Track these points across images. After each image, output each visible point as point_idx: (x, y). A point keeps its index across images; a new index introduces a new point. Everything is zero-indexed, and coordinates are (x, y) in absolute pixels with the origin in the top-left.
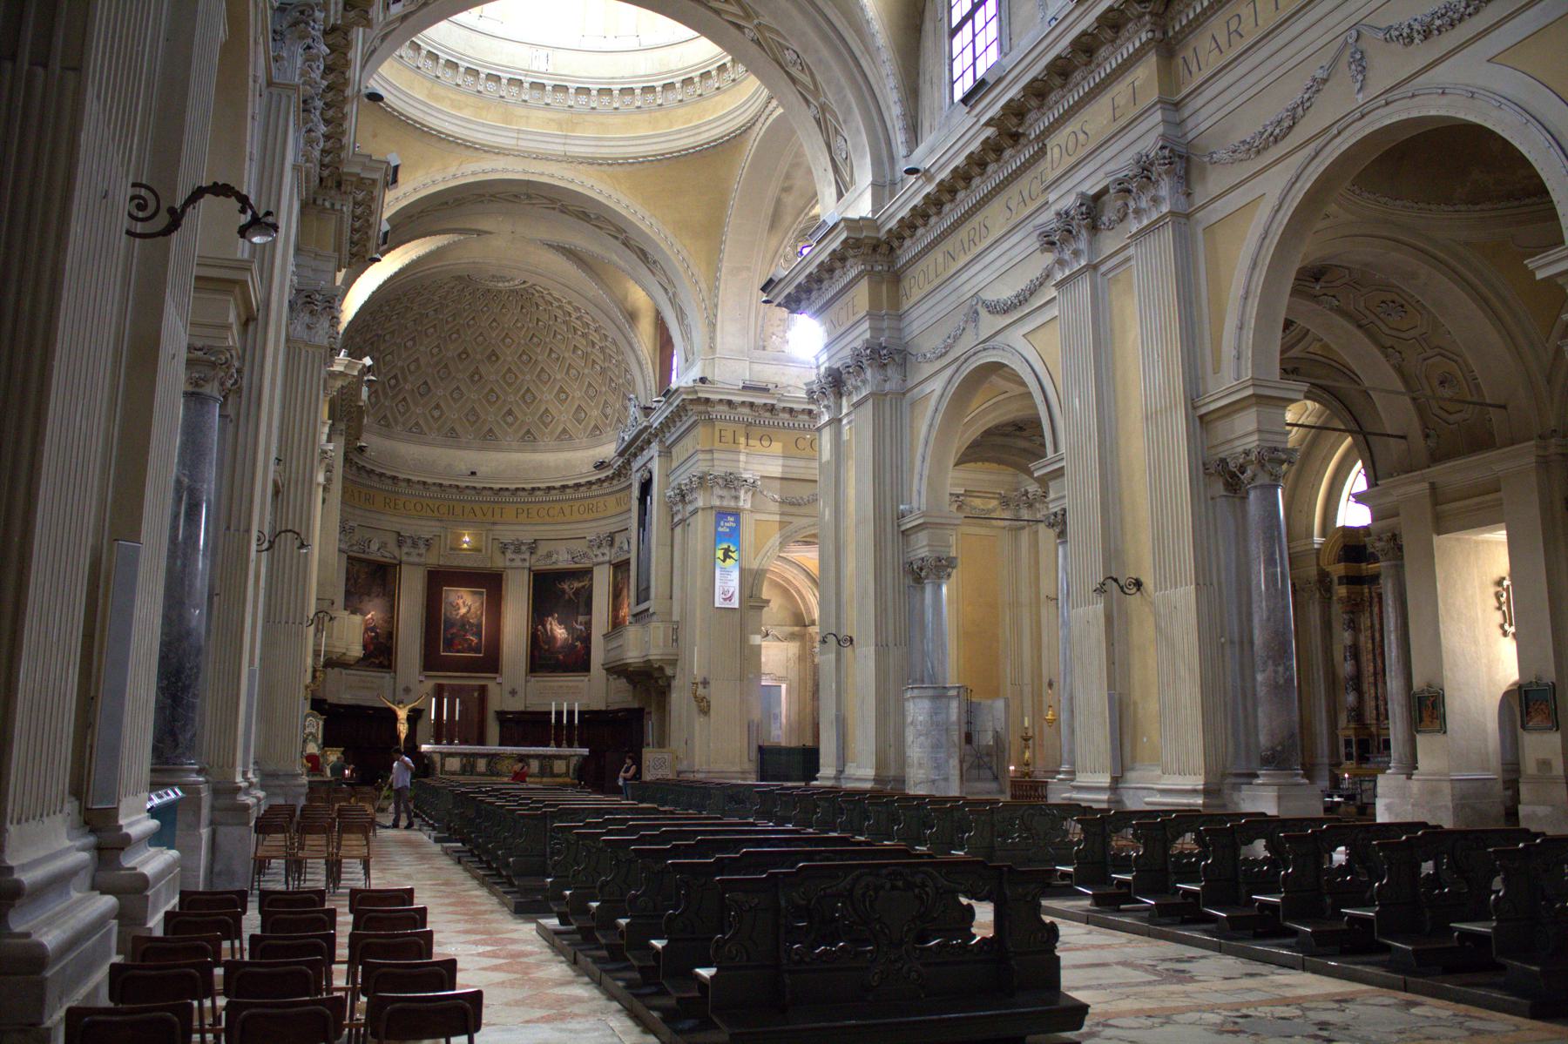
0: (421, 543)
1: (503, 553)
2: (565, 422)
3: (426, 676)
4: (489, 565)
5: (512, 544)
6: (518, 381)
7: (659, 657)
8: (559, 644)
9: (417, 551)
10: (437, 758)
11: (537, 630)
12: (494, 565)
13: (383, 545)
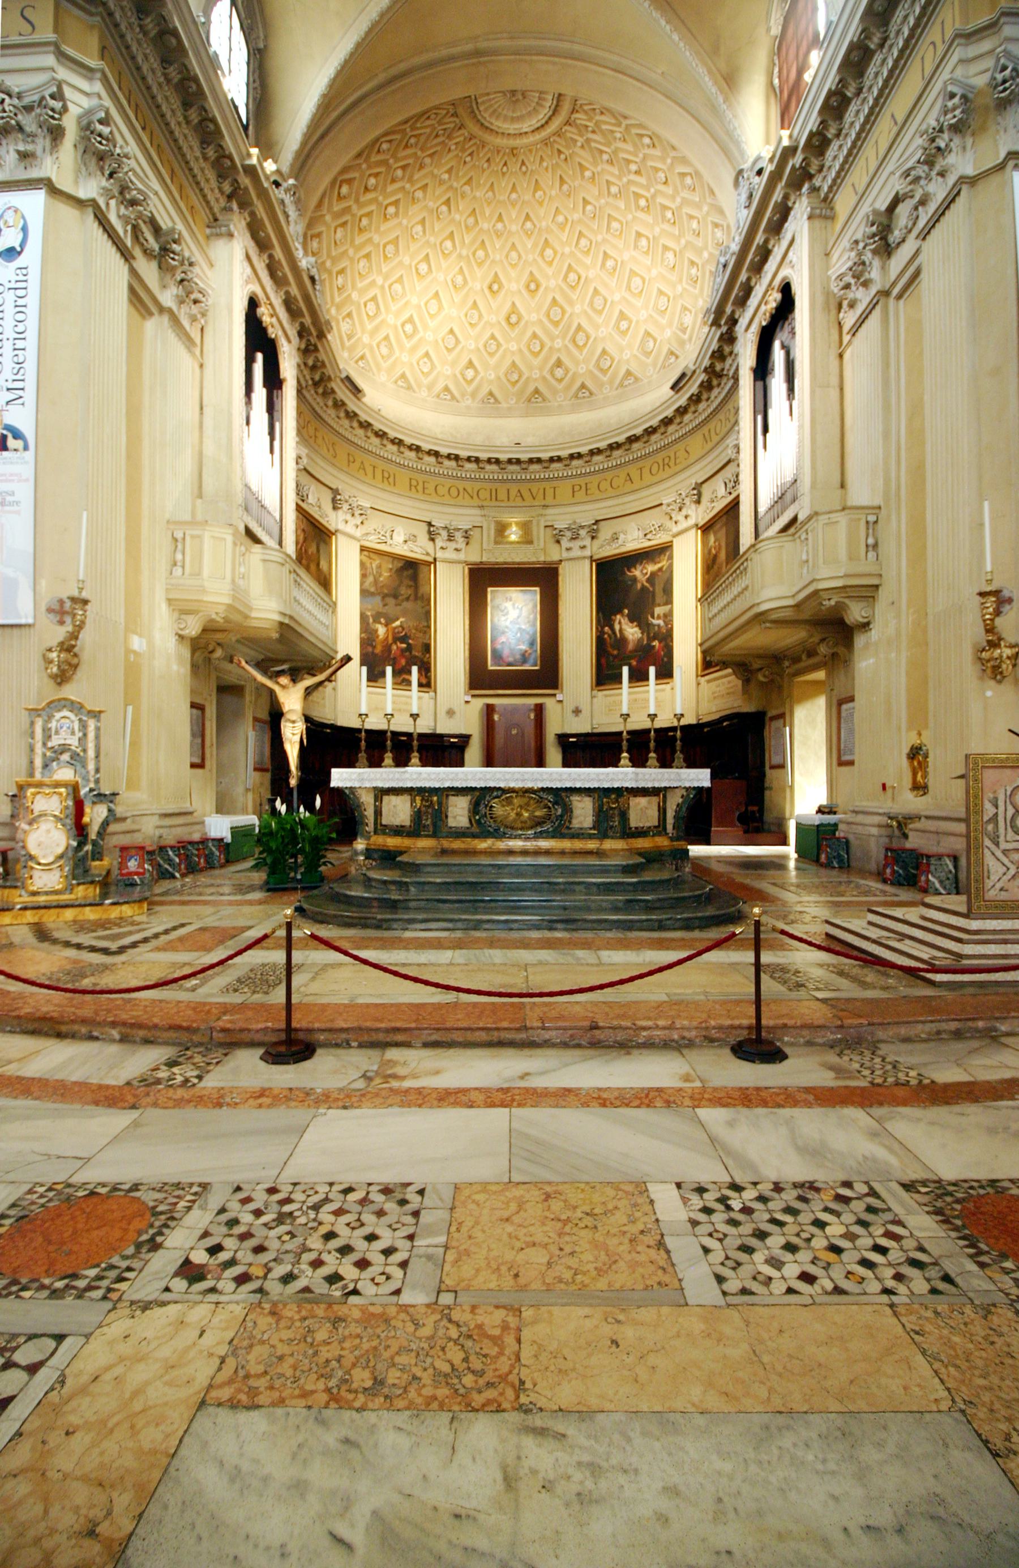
0: (458, 535)
1: (558, 542)
2: (628, 361)
3: (473, 696)
4: (542, 559)
5: (568, 529)
6: (567, 315)
7: (839, 583)
8: (631, 646)
9: (453, 545)
10: (367, 800)
11: (603, 633)
12: (548, 559)
13: (413, 538)
